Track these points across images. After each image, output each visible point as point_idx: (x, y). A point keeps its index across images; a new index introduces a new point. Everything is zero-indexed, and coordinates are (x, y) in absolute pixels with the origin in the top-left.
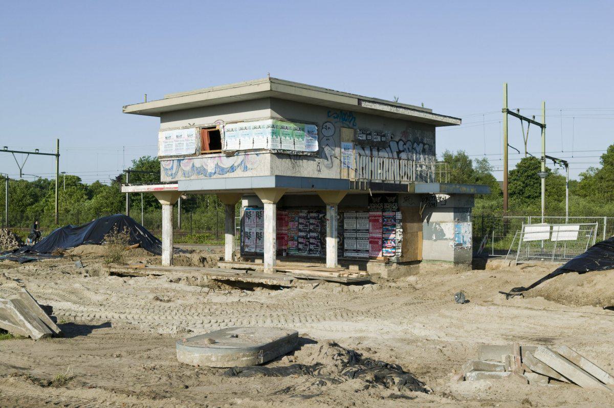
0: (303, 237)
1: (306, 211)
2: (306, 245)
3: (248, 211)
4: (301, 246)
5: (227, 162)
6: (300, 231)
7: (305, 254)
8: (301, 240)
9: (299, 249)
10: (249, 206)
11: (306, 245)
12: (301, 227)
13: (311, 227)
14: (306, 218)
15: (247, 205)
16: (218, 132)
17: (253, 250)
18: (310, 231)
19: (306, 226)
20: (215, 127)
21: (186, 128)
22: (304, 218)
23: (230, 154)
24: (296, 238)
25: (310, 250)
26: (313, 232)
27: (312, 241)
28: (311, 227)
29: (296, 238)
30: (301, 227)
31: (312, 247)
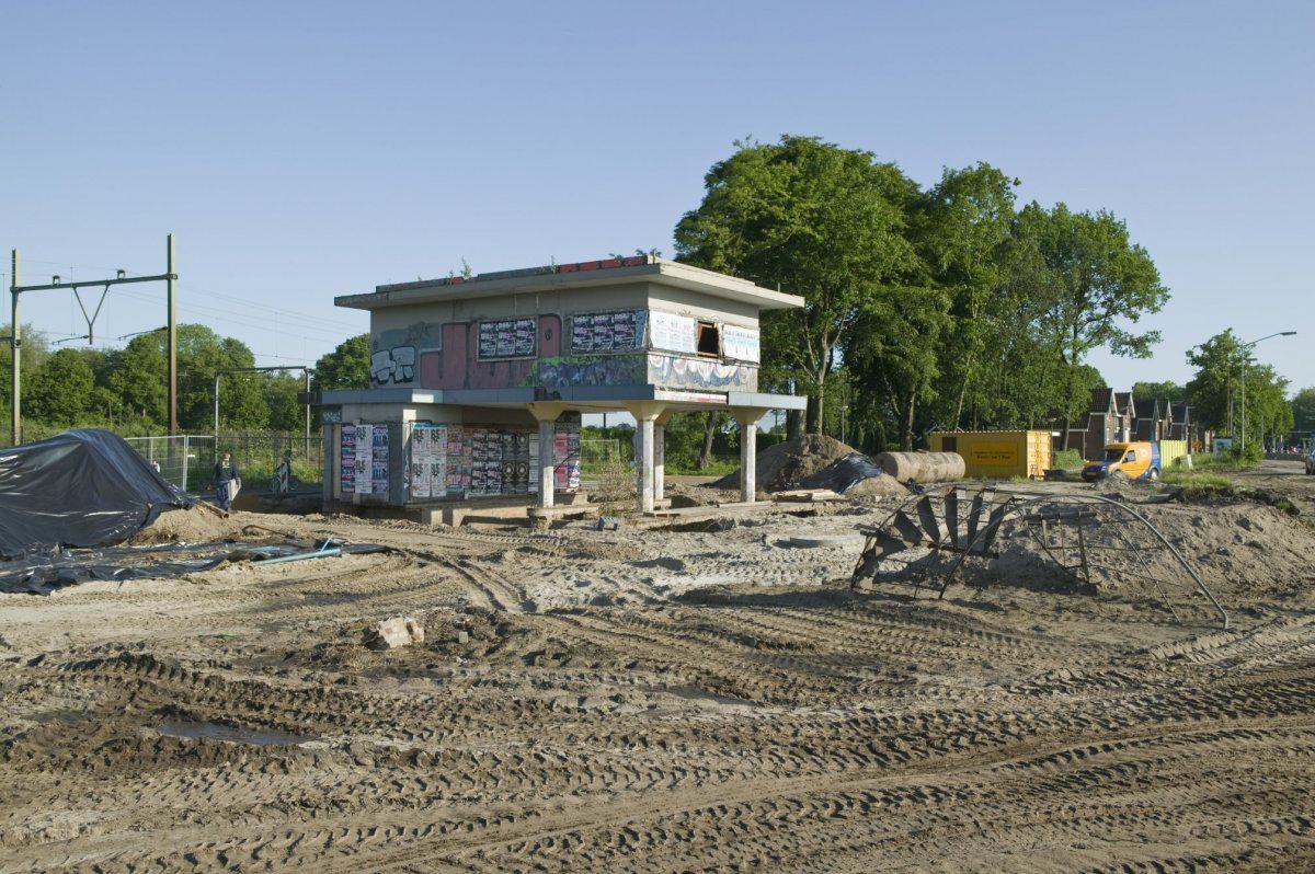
0: (479, 469)
1: (486, 431)
2: (482, 481)
3: (419, 428)
4: (475, 483)
5: (724, 372)
6: (476, 459)
7: (481, 494)
8: (476, 474)
9: (473, 488)
10: (417, 421)
11: (482, 481)
12: (476, 454)
13: (491, 455)
14: (483, 441)
15: (414, 419)
16: (716, 331)
17: (426, 494)
18: (489, 460)
19: (484, 452)
20: (712, 324)
21: (682, 315)
22: (480, 440)
23: (727, 362)
24: (469, 471)
25: (488, 487)
26: (492, 460)
27: (490, 474)
28: (491, 455)
29: (469, 471)
30: (476, 454)
31: (490, 483)
